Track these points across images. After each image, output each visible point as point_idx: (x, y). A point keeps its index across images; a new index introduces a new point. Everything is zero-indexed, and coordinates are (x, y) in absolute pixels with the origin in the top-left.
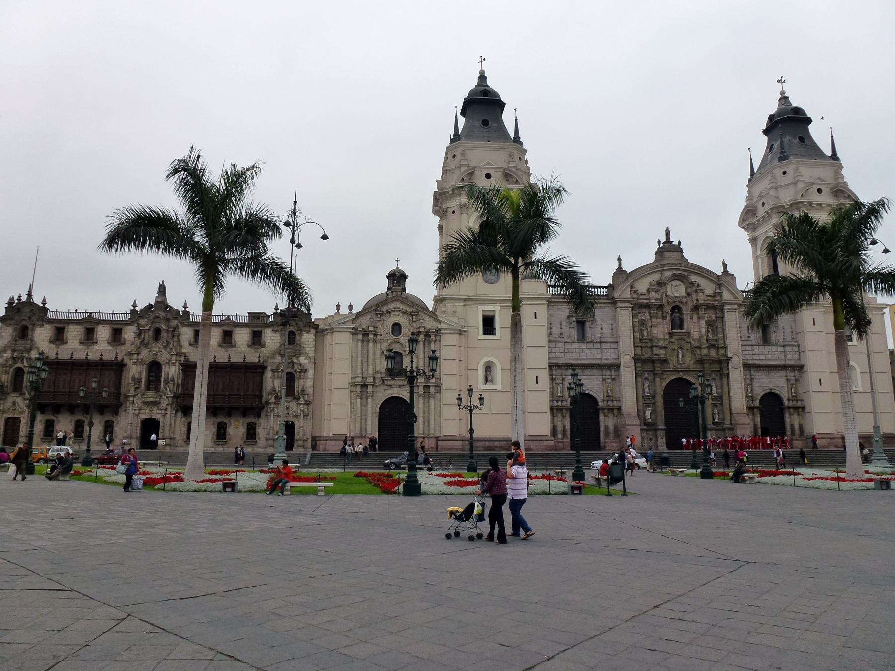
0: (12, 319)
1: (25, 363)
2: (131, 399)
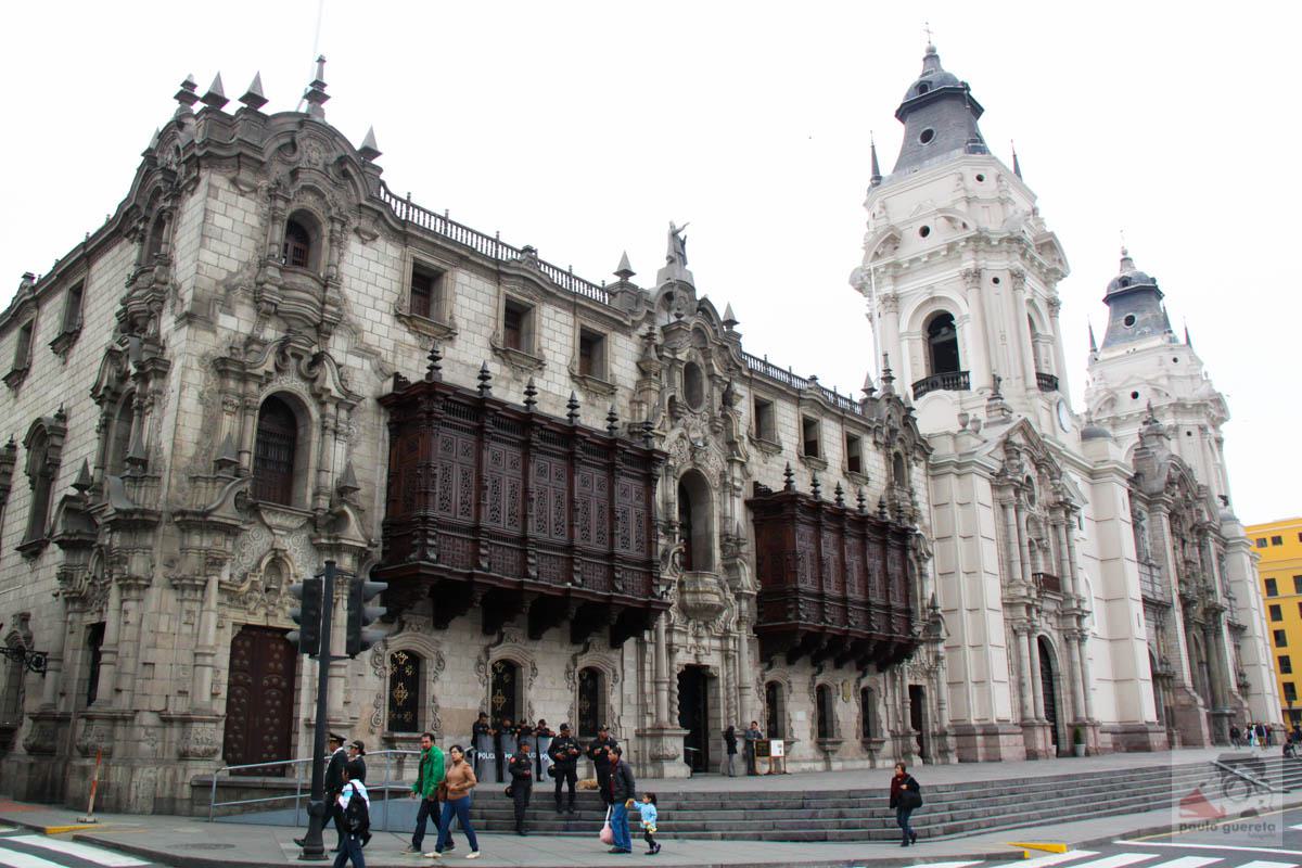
0: (260, 167)
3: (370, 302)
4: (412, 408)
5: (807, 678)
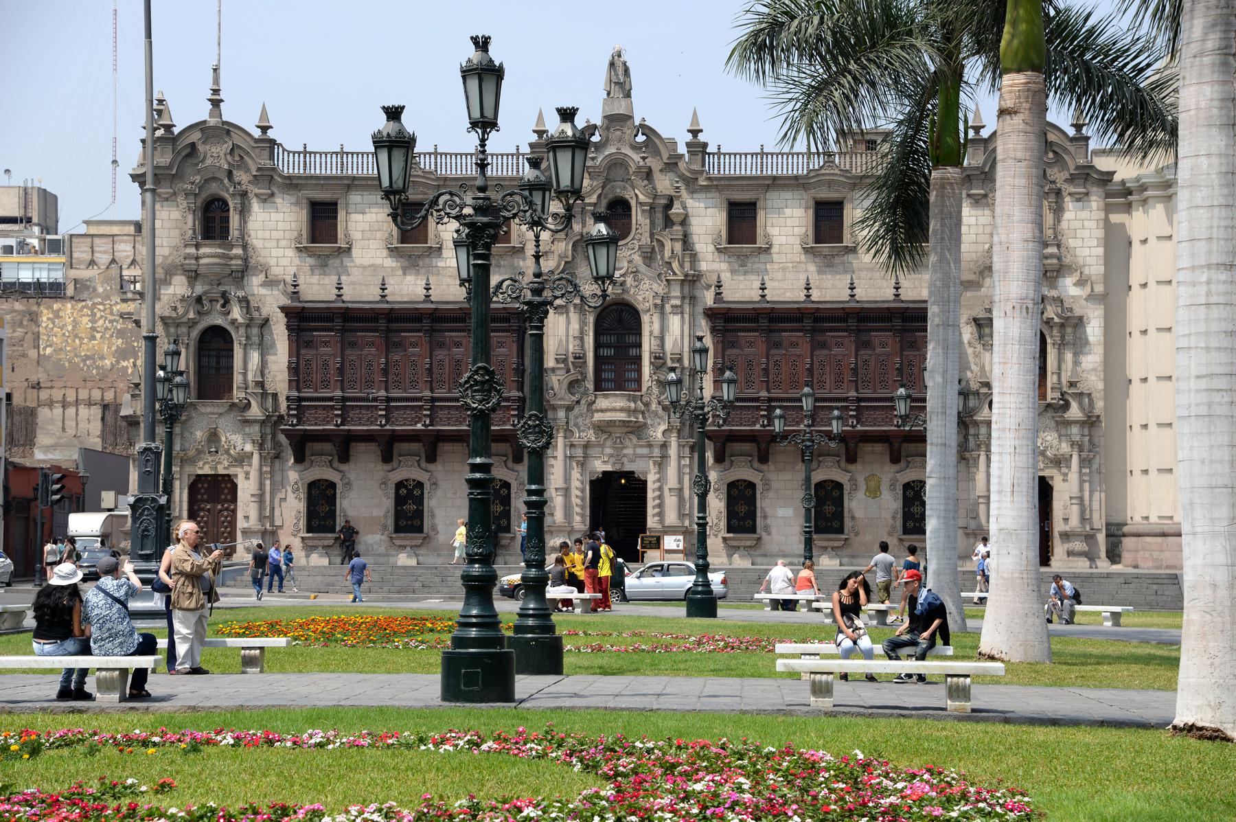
1: (237, 313)
2: (561, 414)
3: (274, 244)
4: (303, 320)
5: (801, 476)
